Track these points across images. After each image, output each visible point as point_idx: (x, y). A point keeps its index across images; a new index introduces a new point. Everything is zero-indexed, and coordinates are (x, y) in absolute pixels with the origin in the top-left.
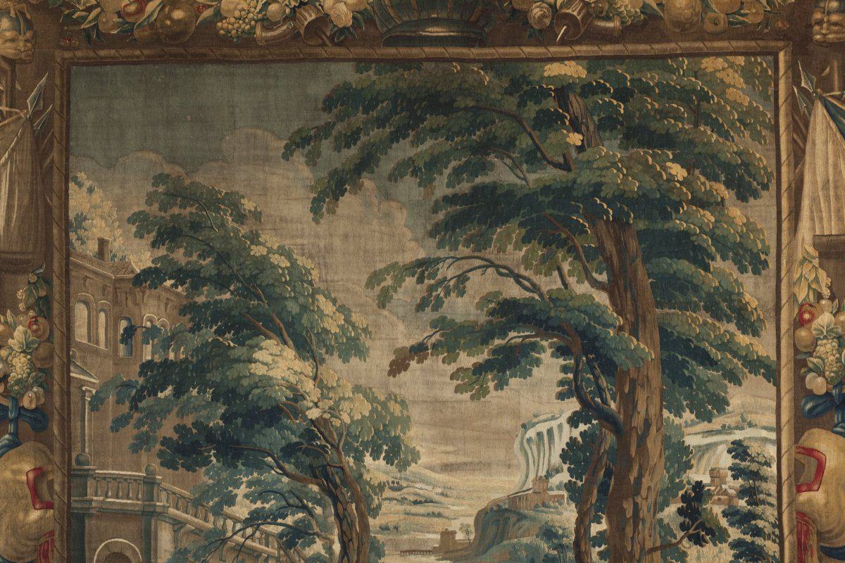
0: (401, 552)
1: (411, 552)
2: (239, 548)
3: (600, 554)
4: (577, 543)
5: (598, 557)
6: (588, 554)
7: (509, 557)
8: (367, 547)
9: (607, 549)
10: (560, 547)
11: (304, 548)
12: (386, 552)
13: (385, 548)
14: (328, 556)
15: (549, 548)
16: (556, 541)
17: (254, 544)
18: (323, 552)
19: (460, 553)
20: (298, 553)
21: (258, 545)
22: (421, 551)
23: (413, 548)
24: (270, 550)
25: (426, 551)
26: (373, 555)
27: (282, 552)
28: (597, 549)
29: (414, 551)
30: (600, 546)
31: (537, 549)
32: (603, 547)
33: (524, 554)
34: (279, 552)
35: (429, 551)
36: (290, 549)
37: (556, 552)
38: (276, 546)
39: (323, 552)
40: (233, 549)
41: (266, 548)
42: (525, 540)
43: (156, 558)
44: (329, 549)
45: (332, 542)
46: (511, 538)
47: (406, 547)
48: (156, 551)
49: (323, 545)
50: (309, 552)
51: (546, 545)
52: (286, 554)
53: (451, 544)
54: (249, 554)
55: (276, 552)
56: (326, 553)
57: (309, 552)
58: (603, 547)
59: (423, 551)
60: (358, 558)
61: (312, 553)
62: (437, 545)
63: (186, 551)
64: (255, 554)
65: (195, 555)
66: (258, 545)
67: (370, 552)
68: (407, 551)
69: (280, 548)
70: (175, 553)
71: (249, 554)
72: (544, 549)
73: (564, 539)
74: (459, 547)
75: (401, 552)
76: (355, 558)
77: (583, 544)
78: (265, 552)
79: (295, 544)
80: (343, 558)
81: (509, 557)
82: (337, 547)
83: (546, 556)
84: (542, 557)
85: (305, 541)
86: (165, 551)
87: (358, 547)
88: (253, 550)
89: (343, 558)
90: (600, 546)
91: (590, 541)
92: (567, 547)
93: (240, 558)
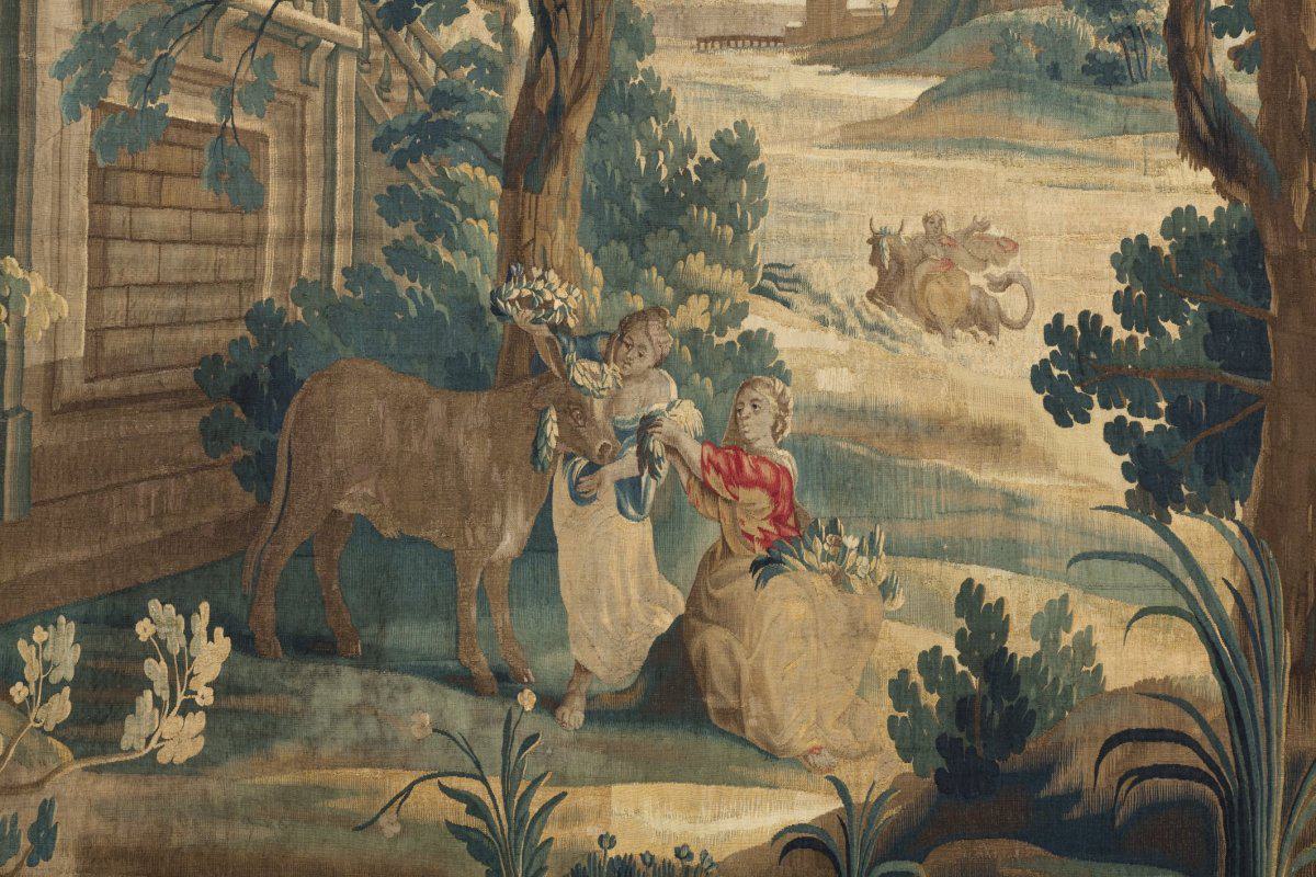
0: (699, 40)
1: (726, 40)
2: (257, 25)
3: (1235, 53)
4: (1174, 25)
5: (1230, 63)
6: (1204, 53)
7: (989, 57)
8: (607, 25)
9: (1253, 43)
10: (1131, 34)
11: (435, 26)
12: (659, 41)
13: (656, 30)
14: (499, 48)
15: (1099, 35)
16: (1117, 18)
17: (298, 15)
18: (486, 37)
19: (859, 45)
20: (418, 40)
21: (310, 19)
22: (752, 39)
23: (733, 30)
24: (342, 30)
25: (767, 39)
26: (621, 49)
27: (375, 38)
28: (1229, 42)
29: (735, 38)
30: (1235, 35)
31: (1066, 38)
32: (1244, 36)
33: (1031, 52)
34: (366, 37)
35: (776, 40)
36: (398, 29)
37: (1117, 48)
38: (359, 19)
39: (486, 37)
40: (241, 27)
41: (331, 26)
42: (1034, 15)
43: (32, 49)
44: (504, 31)
45: (512, 12)
46: (996, 9)
47: (712, 29)
48: (32, 27)
49: (487, 18)
50: (449, 37)
51: (1090, 30)
52: (387, 42)
53: (834, 20)
54: (284, 41)
55: (359, 36)
56: (495, 40)
57: (449, 37)
58: (1244, 36)
59: (760, 39)
60: (582, 54)
61: (456, 40)
62: (798, 24)
63: (114, 31)
64: (301, 43)
65: (139, 43)
66: (310, 19)
67: (613, 38)
68: (713, 39)
69: (369, 25)
70: (85, 37)
71: (284, 41)
72: (1085, 41)
73: (1141, 12)
74: (856, 30)
75: (699, 40)
76: (573, 56)
77: (1190, 28)
78: (330, 37)
79: (411, 17)
80: (541, 53)
81: (989, 57)
82: (525, 26)
83: (1091, 57)
84: (1081, 60)
85: (438, 7)
86: (58, 30)
87: (583, 27)
88: (297, 30)
89: (541, 53)
90: (1235, 35)
91: (1209, 19)
92: (1148, 33)
93: (260, 51)
